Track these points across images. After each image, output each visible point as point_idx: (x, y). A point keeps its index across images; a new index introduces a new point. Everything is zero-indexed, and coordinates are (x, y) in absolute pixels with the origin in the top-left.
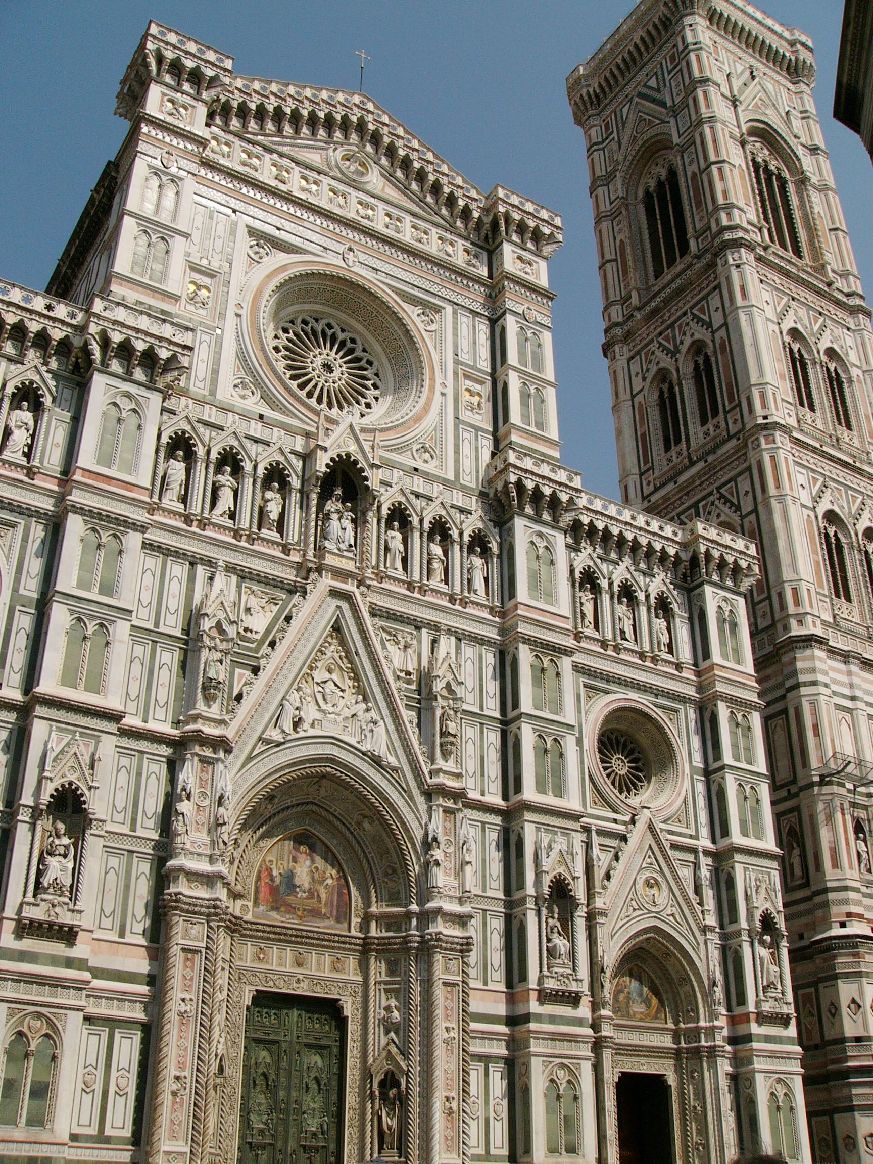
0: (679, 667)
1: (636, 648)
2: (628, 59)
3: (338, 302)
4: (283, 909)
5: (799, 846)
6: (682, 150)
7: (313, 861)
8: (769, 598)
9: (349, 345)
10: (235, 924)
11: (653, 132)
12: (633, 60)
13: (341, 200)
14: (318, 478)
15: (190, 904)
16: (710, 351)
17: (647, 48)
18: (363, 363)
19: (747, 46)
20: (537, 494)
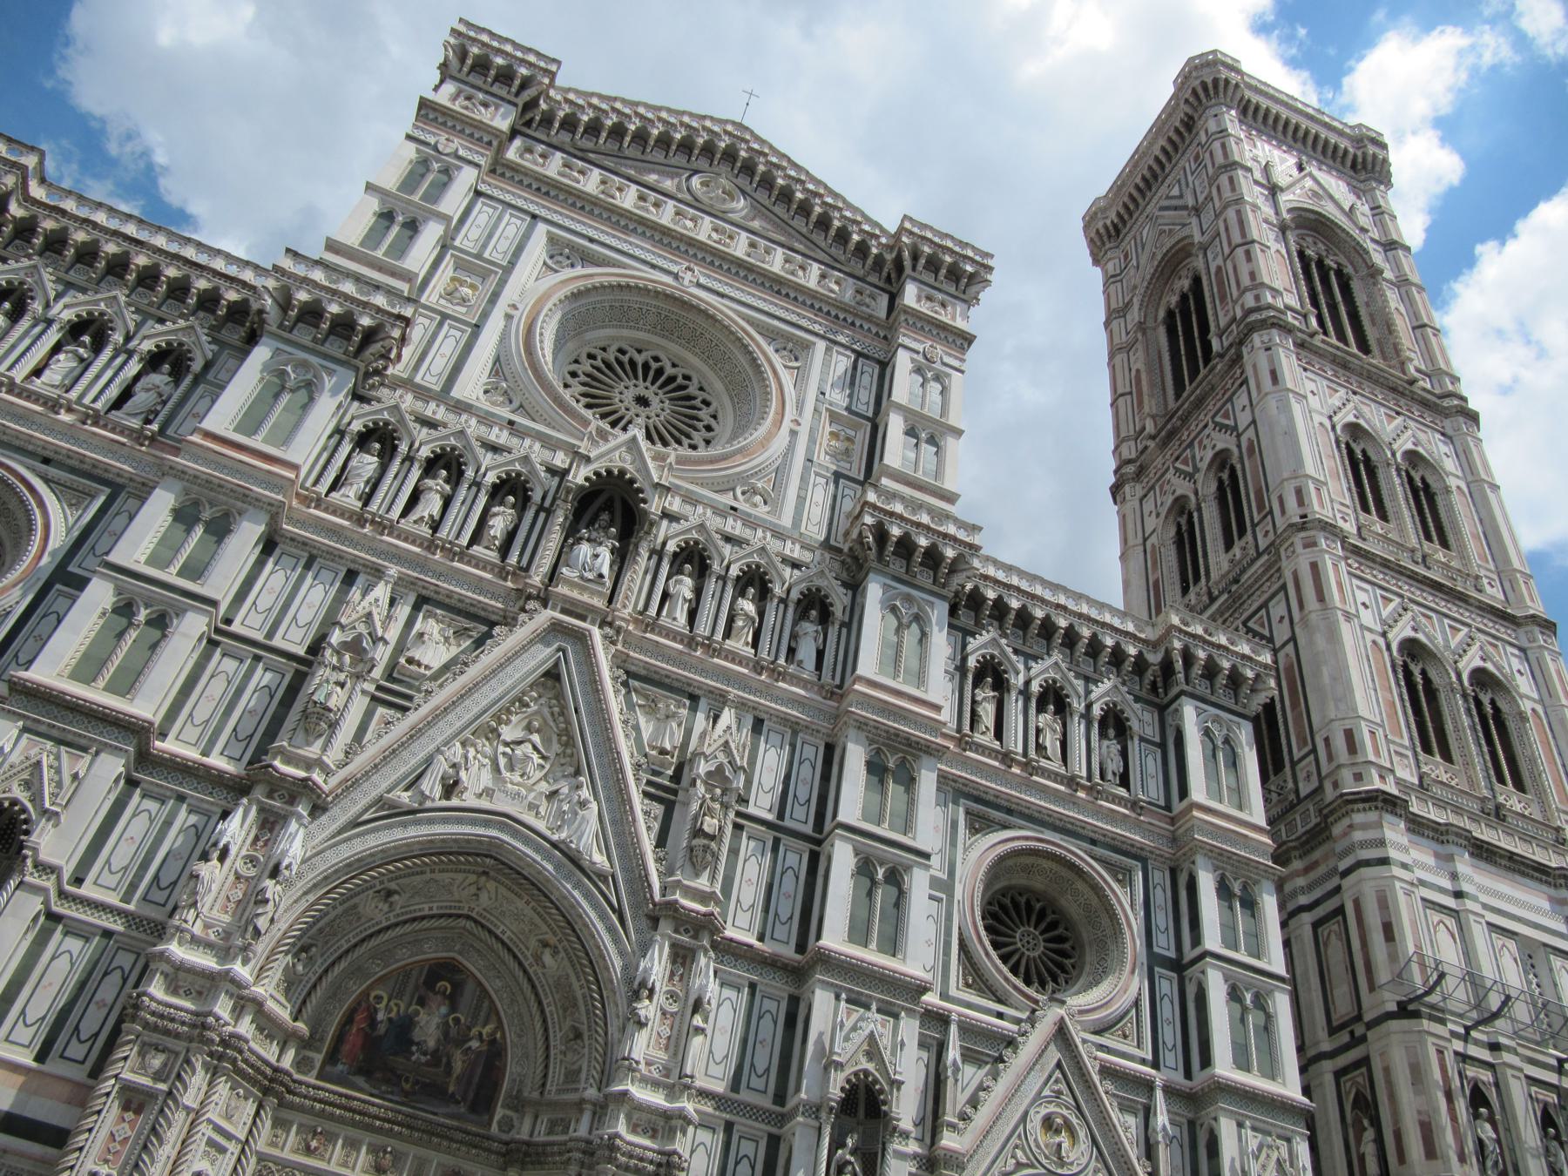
0: (1134, 805)
1: (1062, 771)
2: (1148, 175)
3: (666, 327)
4: (378, 1075)
5: (1372, 1125)
6: (1204, 248)
7: (453, 1008)
8: (1314, 750)
9: (680, 380)
10: (271, 1080)
11: (1173, 241)
12: (1155, 177)
13: (689, 224)
14: (568, 491)
15: (162, 1016)
16: (1235, 460)
17: (1169, 159)
18: (697, 402)
19: (1295, 139)
20: (905, 547)
